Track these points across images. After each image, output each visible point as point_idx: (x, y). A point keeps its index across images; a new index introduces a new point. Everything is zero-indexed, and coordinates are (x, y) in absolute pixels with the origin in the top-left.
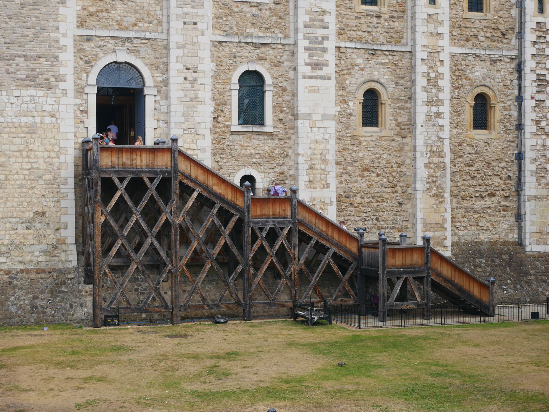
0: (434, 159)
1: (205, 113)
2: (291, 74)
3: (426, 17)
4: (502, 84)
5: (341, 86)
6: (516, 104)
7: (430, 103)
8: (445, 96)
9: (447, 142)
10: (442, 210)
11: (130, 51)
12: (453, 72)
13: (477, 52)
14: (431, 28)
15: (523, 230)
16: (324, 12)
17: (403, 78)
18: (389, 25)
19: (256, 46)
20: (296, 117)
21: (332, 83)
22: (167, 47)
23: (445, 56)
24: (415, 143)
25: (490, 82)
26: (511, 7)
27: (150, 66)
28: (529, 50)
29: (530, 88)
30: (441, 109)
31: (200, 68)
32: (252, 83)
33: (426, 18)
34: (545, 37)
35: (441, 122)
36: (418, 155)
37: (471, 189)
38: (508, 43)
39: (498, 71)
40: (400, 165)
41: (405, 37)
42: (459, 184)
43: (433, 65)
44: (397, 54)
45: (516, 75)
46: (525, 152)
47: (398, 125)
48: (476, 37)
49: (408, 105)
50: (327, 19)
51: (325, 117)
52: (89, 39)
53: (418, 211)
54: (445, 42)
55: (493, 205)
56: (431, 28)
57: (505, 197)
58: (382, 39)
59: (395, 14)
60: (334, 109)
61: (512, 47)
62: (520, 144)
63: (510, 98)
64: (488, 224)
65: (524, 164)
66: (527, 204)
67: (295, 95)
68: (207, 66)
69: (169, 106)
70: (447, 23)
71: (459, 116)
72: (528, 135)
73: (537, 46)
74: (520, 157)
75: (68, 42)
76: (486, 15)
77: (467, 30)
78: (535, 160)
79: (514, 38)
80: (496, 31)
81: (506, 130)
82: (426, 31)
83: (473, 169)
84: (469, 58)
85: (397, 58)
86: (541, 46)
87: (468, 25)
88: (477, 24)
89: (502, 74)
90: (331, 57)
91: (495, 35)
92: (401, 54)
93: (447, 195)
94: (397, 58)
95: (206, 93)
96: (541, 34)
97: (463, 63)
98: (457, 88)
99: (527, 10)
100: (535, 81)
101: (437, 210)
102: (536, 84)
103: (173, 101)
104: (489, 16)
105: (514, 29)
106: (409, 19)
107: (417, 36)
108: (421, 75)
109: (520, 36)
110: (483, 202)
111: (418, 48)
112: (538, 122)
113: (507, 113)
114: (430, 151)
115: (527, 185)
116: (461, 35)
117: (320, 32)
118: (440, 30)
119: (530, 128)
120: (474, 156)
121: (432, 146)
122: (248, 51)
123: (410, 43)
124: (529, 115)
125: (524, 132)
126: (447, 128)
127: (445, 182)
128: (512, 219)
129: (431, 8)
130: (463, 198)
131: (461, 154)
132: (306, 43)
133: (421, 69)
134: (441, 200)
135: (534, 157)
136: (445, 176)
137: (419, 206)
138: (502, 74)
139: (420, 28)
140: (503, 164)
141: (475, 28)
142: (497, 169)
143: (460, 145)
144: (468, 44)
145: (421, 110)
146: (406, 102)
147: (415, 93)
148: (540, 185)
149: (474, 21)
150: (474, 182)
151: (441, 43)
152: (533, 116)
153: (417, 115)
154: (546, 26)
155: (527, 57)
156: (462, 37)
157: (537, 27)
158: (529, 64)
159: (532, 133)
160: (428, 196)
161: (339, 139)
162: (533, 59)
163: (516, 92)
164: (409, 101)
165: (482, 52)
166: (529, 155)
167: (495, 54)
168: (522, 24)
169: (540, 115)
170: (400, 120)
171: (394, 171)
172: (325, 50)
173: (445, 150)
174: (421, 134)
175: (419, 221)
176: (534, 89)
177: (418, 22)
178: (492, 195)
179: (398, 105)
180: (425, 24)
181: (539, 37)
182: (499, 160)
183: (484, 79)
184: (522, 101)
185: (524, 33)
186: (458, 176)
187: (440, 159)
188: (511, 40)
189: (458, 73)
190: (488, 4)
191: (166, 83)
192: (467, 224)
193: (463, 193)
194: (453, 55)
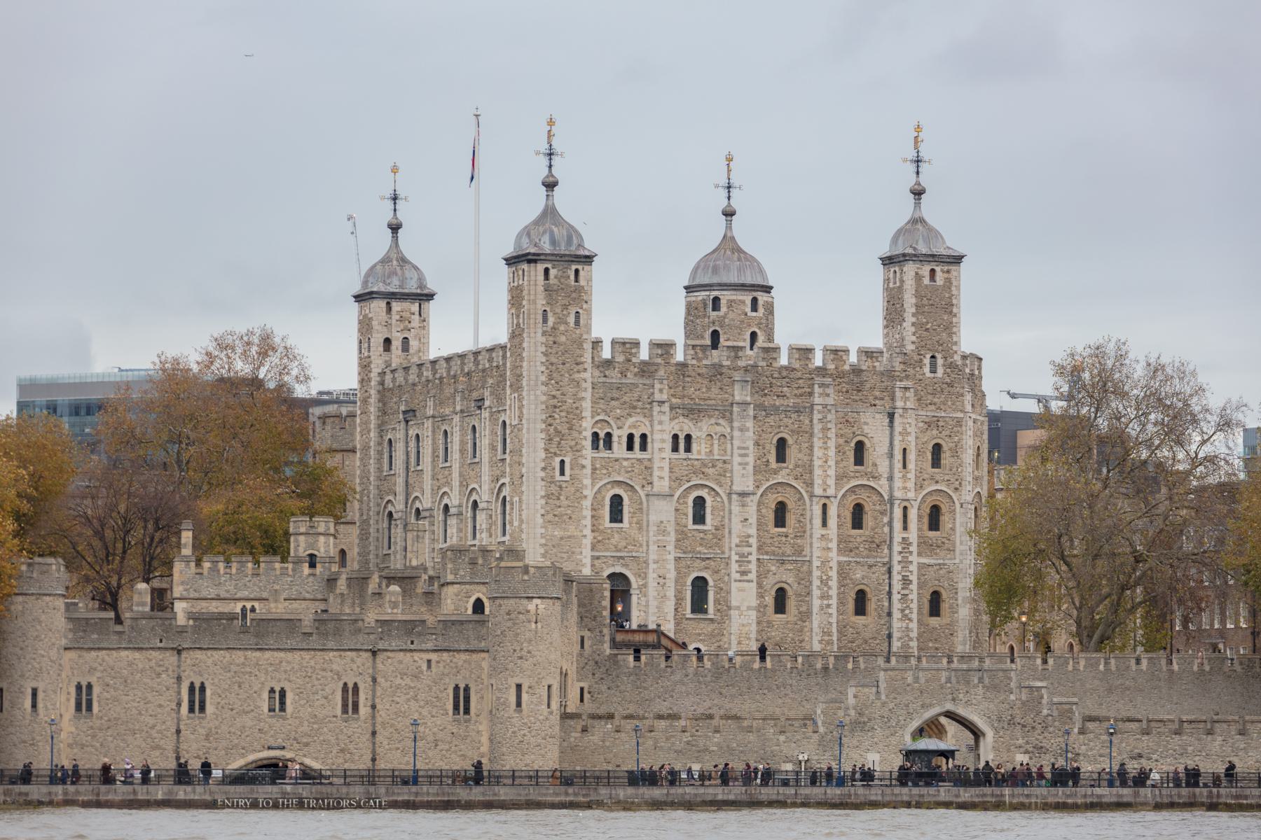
1: (670, 606)
2: (726, 578)
5: (760, 585)
7: (822, 597)
8: (834, 592)
9: (835, 625)
11: (623, 565)
14: (824, 544)
16: (749, 536)
19: (703, 560)
20: (729, 608)
21: (754, 585)
22: (646, 562)
23: (834, 564)
27: (635, 575)
29: (897, 586)
31: (668, 576)
32: (700, 586)
35: (830, 611)
40: (801, 642)
50: (751, 540)
51: (749, 608)
52: (598, 558)
56: (824, 544)
58: (788, 552)
60: (754, 602)
62: (890, 627)
67: (729, 592)
68: (672, 575)
69: (647, 602)
72: (895, 620)
74: (890, 636)
75: (588, 561)
81: (880, 616)
88: (859, 540)
90: (753, 567)
95: (671, 593)
103: (651, 598)
109: (890, 548)
111: (814, 559)
112: (902, 611)
117: (746, 550)
119: (896, 615)
122: (698, 563)
124: (897, 605)
132: (737, 558)
133: (816, 573)
139: (816, 544)
145: (816, 603)
152: (899, 606)
155: (895, 563)
158: (897, 568)
161: (759, 623)
166: (896, 635)
167: (871, 561)
172: (749, 562)
177: (814, 540)
191: (645, 586)
194: (839, 563)
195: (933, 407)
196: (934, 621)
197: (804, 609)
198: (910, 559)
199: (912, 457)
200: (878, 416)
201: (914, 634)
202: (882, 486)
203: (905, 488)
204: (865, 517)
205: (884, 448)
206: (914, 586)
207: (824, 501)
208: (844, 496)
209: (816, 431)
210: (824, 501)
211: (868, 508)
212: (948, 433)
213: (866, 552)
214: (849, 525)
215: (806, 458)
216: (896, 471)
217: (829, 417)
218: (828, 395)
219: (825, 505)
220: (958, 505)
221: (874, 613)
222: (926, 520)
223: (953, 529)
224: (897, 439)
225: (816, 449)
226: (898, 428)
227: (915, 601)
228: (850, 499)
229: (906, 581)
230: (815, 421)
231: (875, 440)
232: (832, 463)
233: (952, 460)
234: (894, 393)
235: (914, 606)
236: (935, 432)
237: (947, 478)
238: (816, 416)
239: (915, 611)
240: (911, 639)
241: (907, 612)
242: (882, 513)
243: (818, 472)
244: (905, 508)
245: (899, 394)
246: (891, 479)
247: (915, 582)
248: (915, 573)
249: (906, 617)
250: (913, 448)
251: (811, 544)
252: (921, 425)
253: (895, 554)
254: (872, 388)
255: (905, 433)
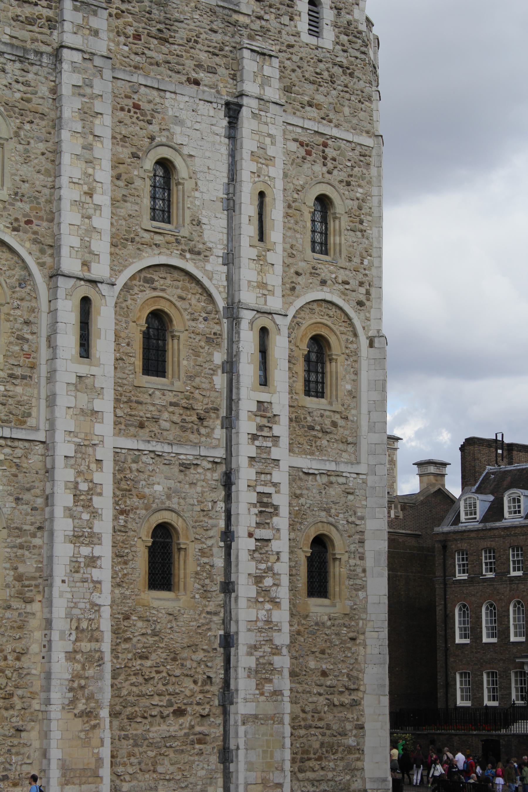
0: (83, 644)
3: (73, 379)
4: (198, 508)
6: (222, 544)
7: (77, 538)
8: (104, 526)
9: (106, 612)
10: (95, 742)
12: (117, 482)
13: (158, 448)
15: (233, 780)
17: (28, 490)
18: (6, 390)
23: (105, 453)
24: (51, 612)
25: (179, 504)
26: (214, 371)
28: (245, 449)
29: (245, 518)
30: (97, 551)
33: (74, 382)
34: (270, 428)
35: (96, 574)
36: (55, 636)
37: (145, 702)
38: (208, 436)
39: (192, 484)
41: (34, 413)
42: (124, 692)
43: (83, 468)
44: (20, 444)
45: (222, 494)
46: (237, 633)
47: (19, 578)
48: (156, 420)
49: (37, 541)
53: (53, 744)
54: (105, 428)
55: (182, 733)
56: (83, 400)
57: (202, 716)
59: (18, 372)
61: (215, 442)
63: (211, 533)
64: (172, 769)
65: (237, 655)
66: (242, 729)
70: (109, 395)
71: (126, 563)
72: (242, 603)
73: (257, 443)
74: (228, 642)
76: (172, 384)
77: (140, 407)
78: (255, 648)
79: (219, 427)
80: (188, 413)
81: (206, 593)
82: (73, 406)
83: (148, 663)
84: (144, 458)
85: (19, 452)
86: (265, 444)
87: (145, 398)
89: (199, 489)
91: (188, 419)
92: (27, 444)
93: (104, 713)
94: (19, 452)
96: (264, 422)
97: (134, 466)
98: (122, 512)
99: (242, 379)
100: (255, 505)
101: (86, 743)
102: (255, 511)
104: (178, 385)
105: (218, 410)
106: (43, 381)
107: (57, 414)
108: (62, 485)
109: (229, 423)
110: (164, 727)
111: (59, 436)
112: (258, 579)
113: (206, 560)
114: (77, 628)
115: (241, 694)
116: (130, 415)
118: (98, 405)
119: (245, 589)
120: (151, 640)
121: (79, 620)
123: (43, 425)
124: (245, 567)
125: (237, 598)
126: (107, 587)
127: (101, 689)
128: (214, 759)
129: (83, 364)
130: (131, 718)
131: (128, 635)
133: (64, 474)
134: (93, 723)
135: (253, 642)
136: (101, 678)
137: (56, 735)
138: (199, 489)
139: (64, 400)
140: (200, 655)
141: (154, 405)
142: (188, 664)
143: (127, 618)
144: (141, 432)
145: (63, 551)
146: (34, 536)
147: (52, 519)
148: (262, 694)
149: (153, 393)
150: (149, 689)
151: (99, 429)
153: (55, 560)
154: (271, 408)
156: (132, 419)
157: (259, 409)
158: (245, 474)
159: (249, 600)
160: (71, 716)
162: (251, 465)
163: (222, 524)
164: (39, 534)
165: (167, 448)
166: (245, 639)
167: (187, 453)
168: (232, 402)
169: (263, 566)
170: (21, 569)
171: (8, 667)
173: (102, 628)
174: (61, 596)
175: (54, 765)
176: (254, 520)
177: (60, 389)
178: (180, 713)
179: (19, 541)
180: (73, 393)
181: (260, 428)
182: (193, 647)
183: (169, 497)
184: (232, 540)
185: (237, 418)
186: (122, 677)
187: (94, 645)
188: (213, 429)
189: (125, 486)
190: (176, 364)
192: (136, 768)
193: (129, 710)
195: (312, 112)
196: (317, 607)
197: (29, 567)
198: (275, 453)
199: (276, 213)
200: (203, 108)
201: (283, 638)
202: (212, 273)
203: (262, 285)
204: (171, 346)
205: (214, 187)
206: (282, 521)
207: (85, 290)
208: (127, 287)
209: (67, 114)
210: (85, 290)
211: (179, 323)
212: (343, 176)
213: (173, 433)
214: (139, 363)
215: (40, 180)
216: (245, 242)
217: (99, 86)
218: (96, 33)
219: (86, 302)
220: (364, 342)
221: (193, 585)
222: (300, 367)
223: (353, 395)
224: (247, 167)
225: (66, 159)
226: (248, 144)
227: (285, 557)
228: (141, 297)
229: (266, 508)
230: (66, 90)
231: (198, 163)
232: (103, 199)
233: (351, 237)
234: (239, 61)
235: (282, 568)
236: (318, 168)
237: (342, 276)
238: (69, 78)
239: (285, 580)
240: (276, 651)
241: (268, 582)
242: (209, 341)
243: (69, 216)
244: (264, 331)
245: (250, 63)
246: (230, 259)
247: (284, 511)
248: (285, 488)
249: (265, 596)
250: (279, 196)
251: (51, 401)
252: (293, 146)
253: (243, 439)
254: (192, 41)
255: (262, 157)
